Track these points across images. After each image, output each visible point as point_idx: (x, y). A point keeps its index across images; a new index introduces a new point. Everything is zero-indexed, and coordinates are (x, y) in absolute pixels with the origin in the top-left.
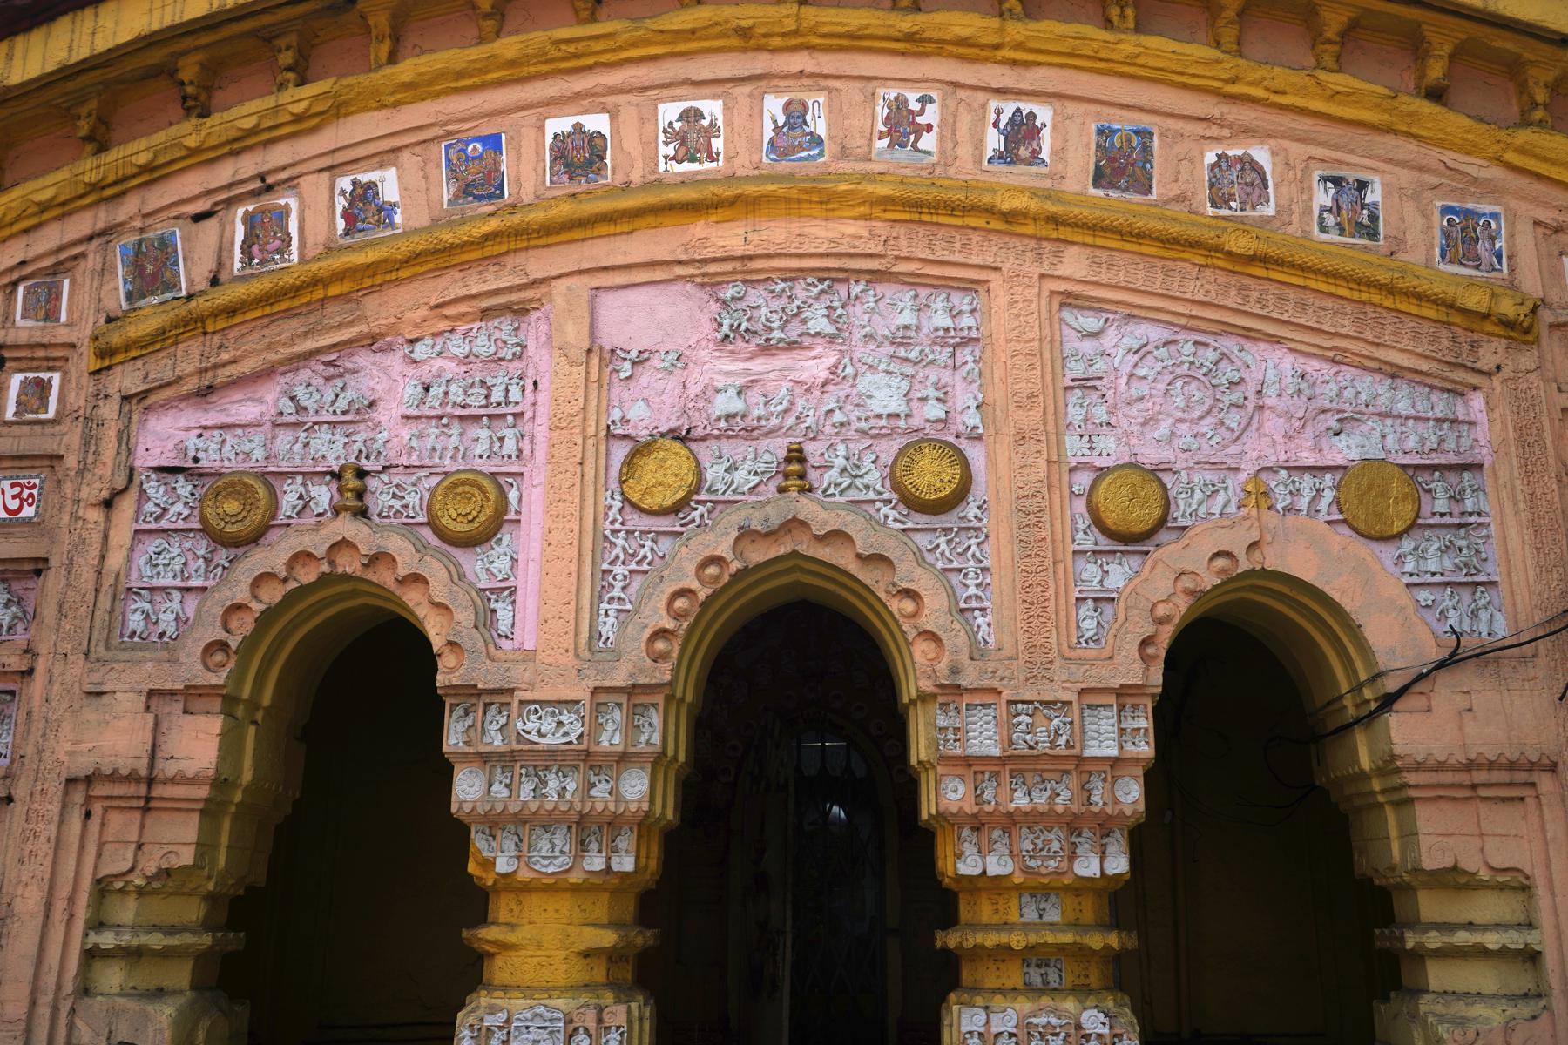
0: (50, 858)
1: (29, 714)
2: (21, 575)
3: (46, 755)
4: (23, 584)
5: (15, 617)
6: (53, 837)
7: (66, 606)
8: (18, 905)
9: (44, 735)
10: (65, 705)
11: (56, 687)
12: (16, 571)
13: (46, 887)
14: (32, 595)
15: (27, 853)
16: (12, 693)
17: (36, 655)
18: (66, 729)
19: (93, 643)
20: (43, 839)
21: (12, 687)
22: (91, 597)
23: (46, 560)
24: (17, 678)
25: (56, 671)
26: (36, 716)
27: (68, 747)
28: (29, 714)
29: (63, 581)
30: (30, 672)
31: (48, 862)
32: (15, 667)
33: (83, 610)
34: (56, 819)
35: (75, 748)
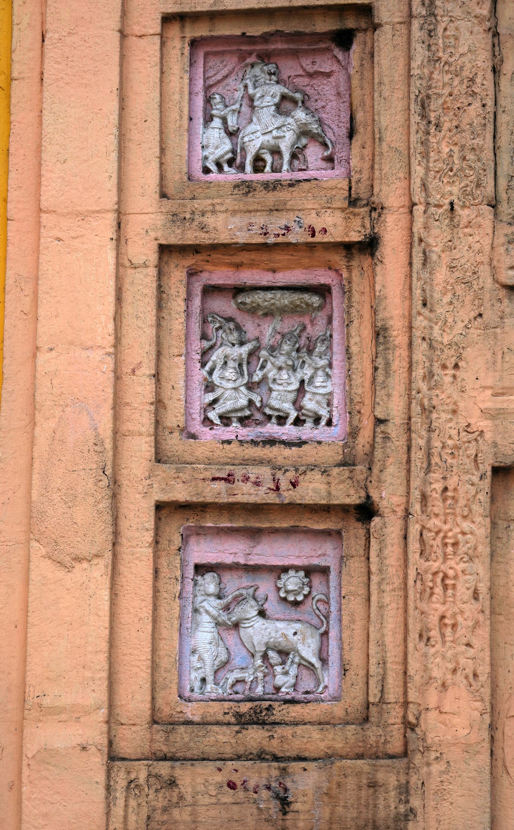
0: (484, 632)
1: (380, 334)
2: (302, 44)
3: (440, 418)
4: (306, 63)
5: (304, 132)
6: (483, 588)
7: (434, 105)
8: (433, 727)
9: (429, 375)
10: (466, 313)
11: (441, 275)
12: (297, 36)
13: (486, 692)
14: (326, 89)
15: (434, 620)
16: (323, 291)
17: (376, 209)
18: (476, 360)
19: (503, 182)
20: (463, 592)
21: (322, 277)
22: (485, 82)
23: (366, 11)
24: (338, 259)
25: (437, 238)
26: (398, 336)
27: (486, 400)
28: (380, 334)
29: (420, 53)
30: (370, 245)
31: (481, 639)
32: (337, 235)
33: (474, 111)
34: (484, 550)
35: (501, 402)
